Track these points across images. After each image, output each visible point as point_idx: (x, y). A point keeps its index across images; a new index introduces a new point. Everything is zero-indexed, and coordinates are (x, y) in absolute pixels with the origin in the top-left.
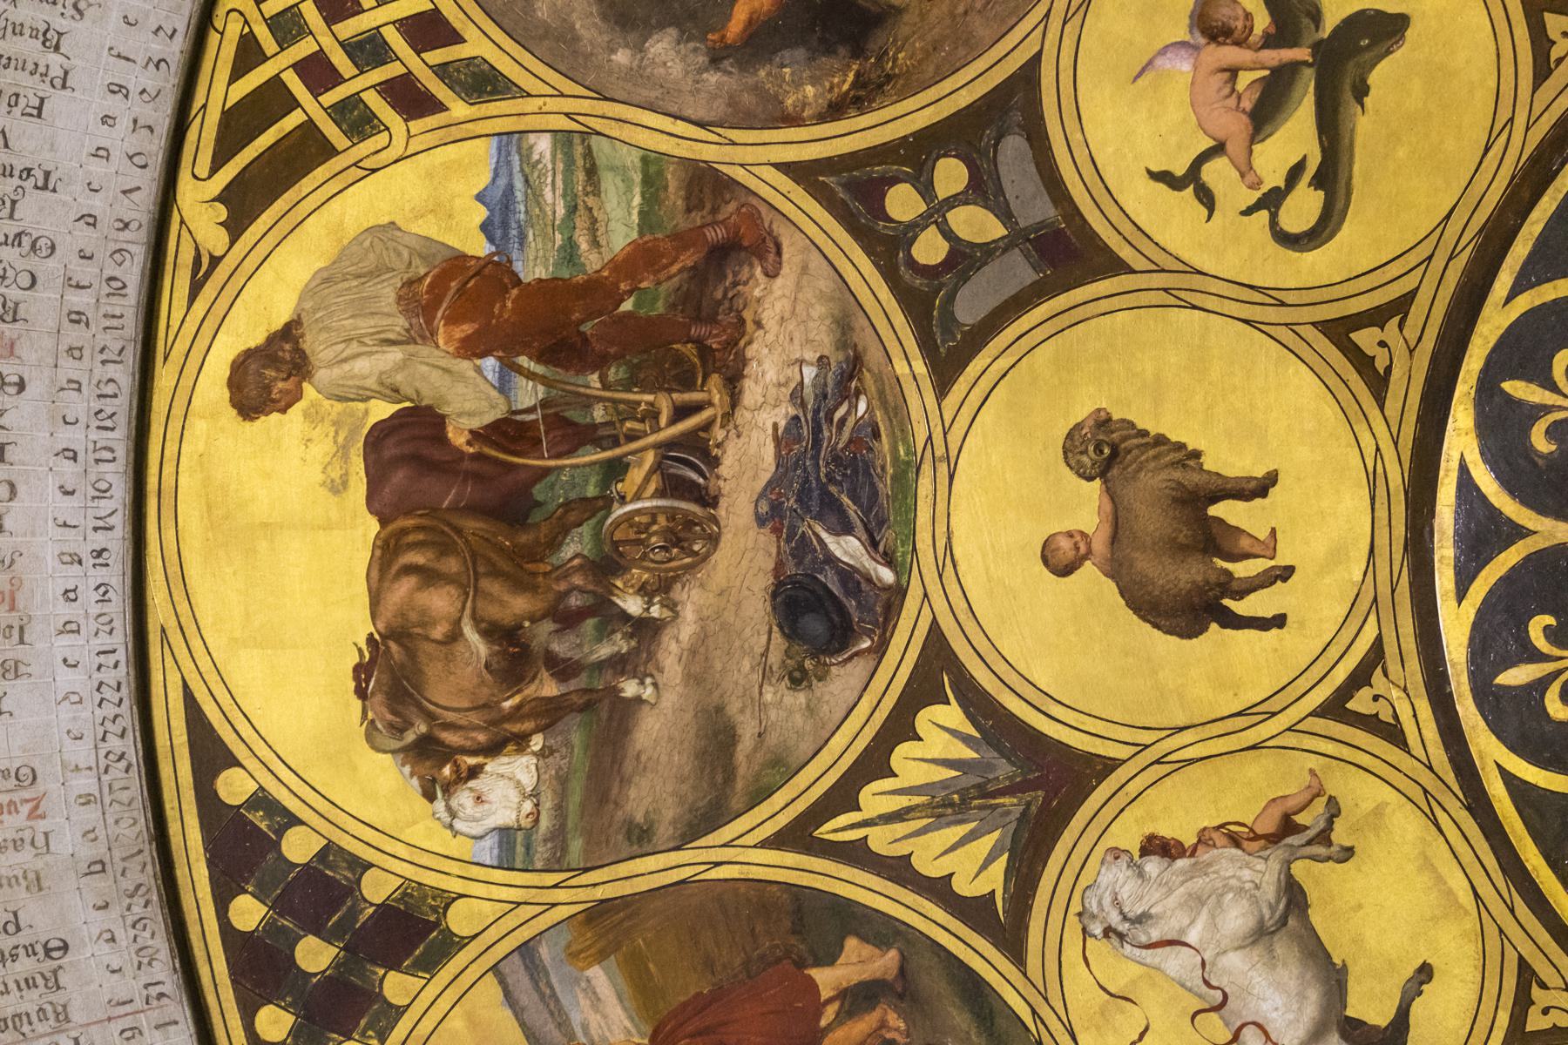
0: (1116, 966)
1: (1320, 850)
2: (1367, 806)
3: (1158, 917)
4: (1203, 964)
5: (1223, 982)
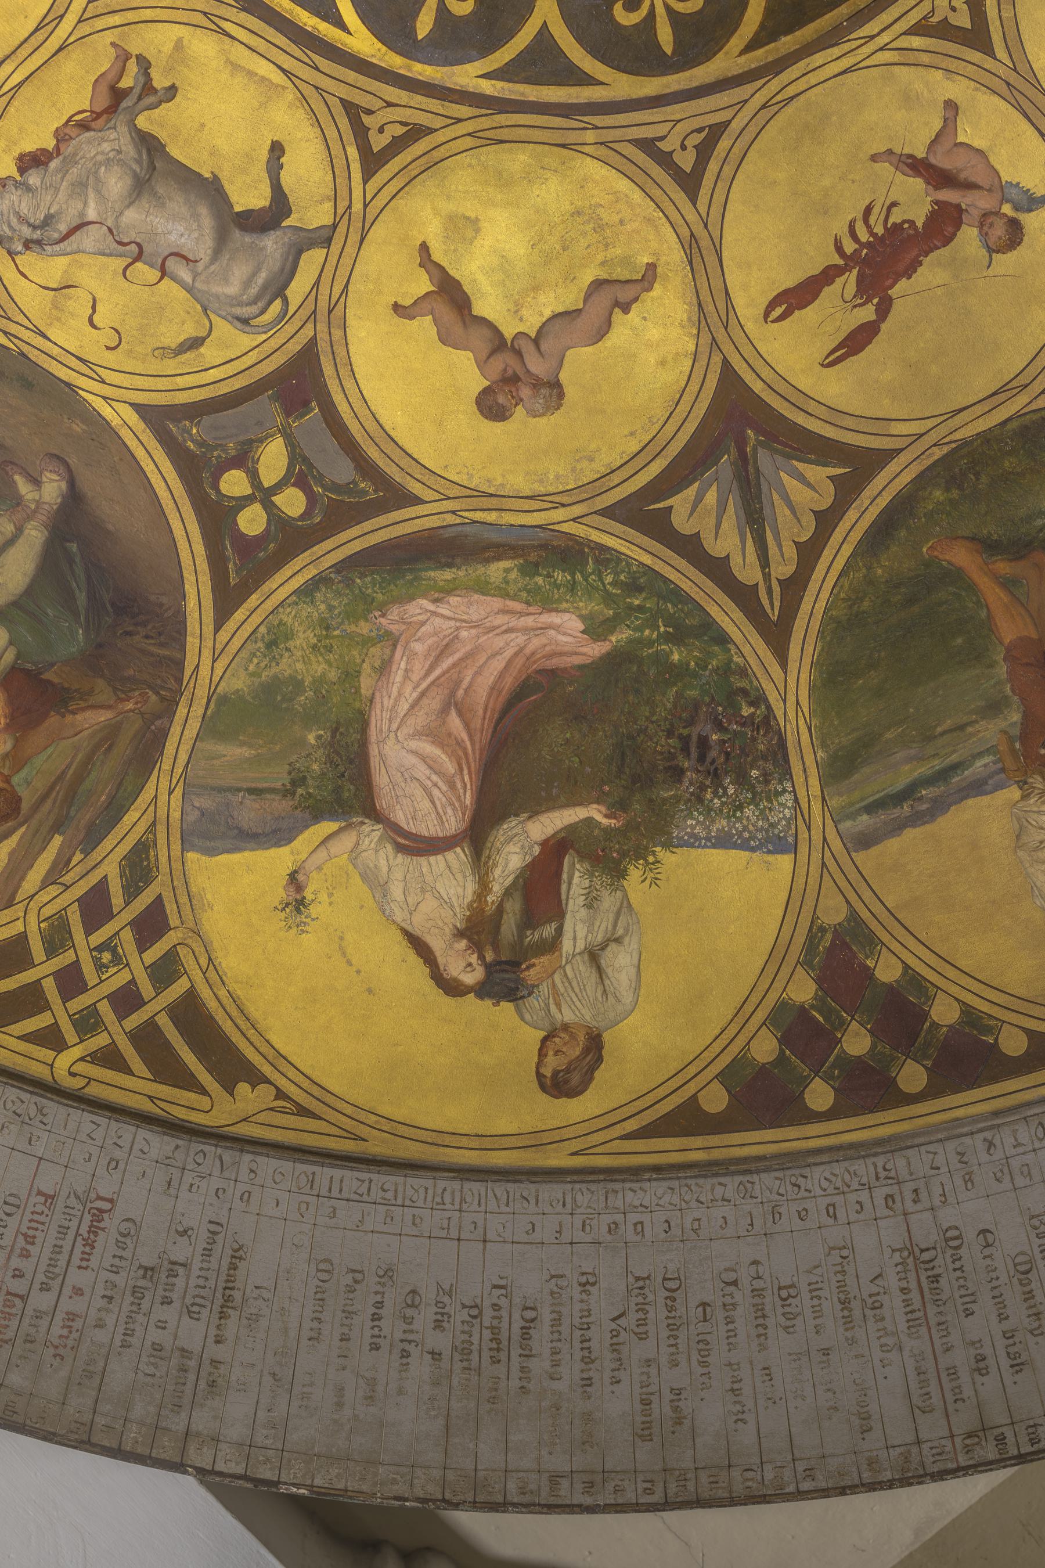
0: (51, 268)
1: (151, 99)
2: (168, 48)
3: (59, 213)
4: (110, 230)
5: (133, 236)
